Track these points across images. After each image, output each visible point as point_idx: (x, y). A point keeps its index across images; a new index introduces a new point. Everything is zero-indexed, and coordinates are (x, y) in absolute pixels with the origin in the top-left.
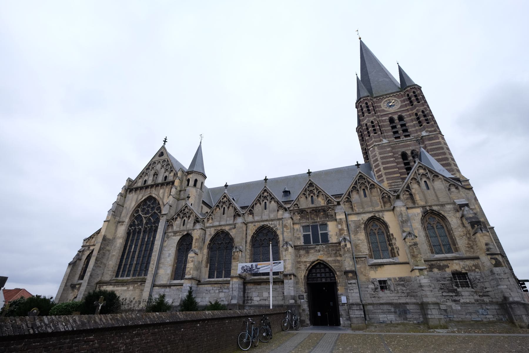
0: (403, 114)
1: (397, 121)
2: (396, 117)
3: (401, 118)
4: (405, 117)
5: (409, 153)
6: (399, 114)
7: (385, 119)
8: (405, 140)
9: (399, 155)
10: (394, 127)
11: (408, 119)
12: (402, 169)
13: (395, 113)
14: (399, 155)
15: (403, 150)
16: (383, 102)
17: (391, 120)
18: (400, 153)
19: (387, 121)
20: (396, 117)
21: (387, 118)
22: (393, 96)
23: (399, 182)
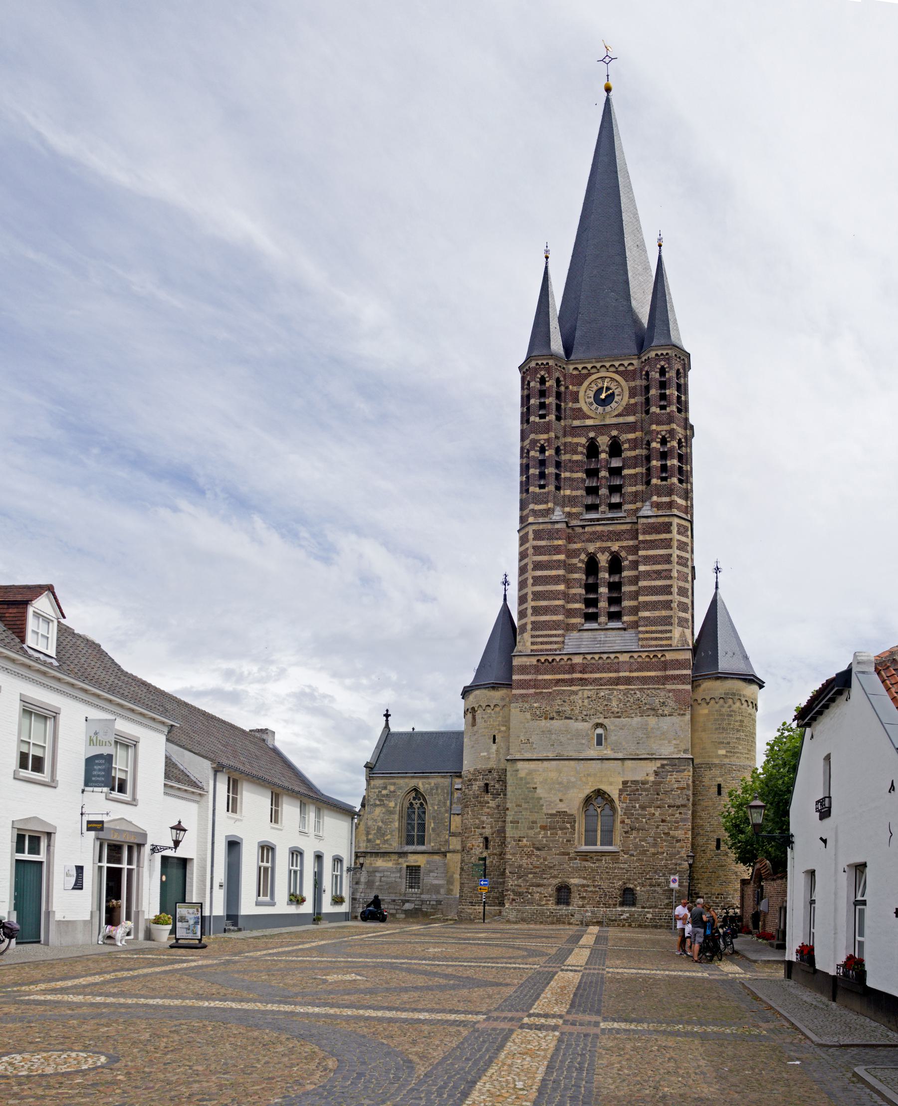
0: (624, 437)
2: (603, 441)
4: (626, 446)
5: (603, 559)
6: (614, 433)
7: (577, 444)
8: (608, 519)
9: (581, 561)
10: (592, 473)
11: (633, 453)
12: (577, 602)
13: (602, 429)
14: (580, 562)
15: (591, 548)
16: (586, 383)
17: (592, 450)
18: (583, 556)
19: (580, 449)
20: (603, 441)
21: (583, 440)
22: (613, 369)
23: (555, 636)
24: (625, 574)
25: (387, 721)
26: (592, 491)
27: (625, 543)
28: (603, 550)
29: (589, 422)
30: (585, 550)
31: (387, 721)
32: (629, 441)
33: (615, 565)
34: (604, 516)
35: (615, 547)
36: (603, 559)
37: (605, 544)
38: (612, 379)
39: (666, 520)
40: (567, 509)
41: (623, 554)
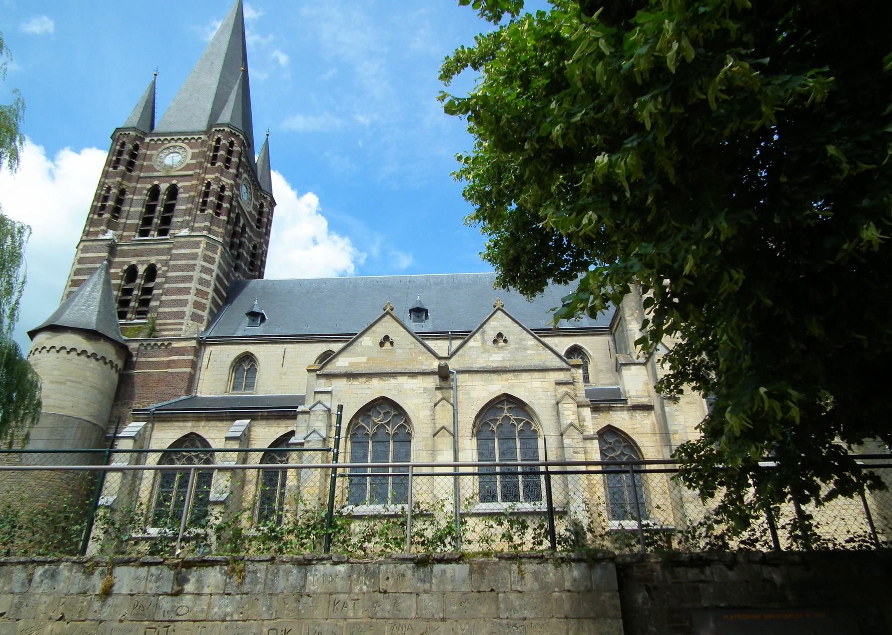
0: (179, 185)
1: (163, 197)
2: (164, 187)
3: (173, 192)
4: (181, 190)
5: (141, 269)
6: (174, 182)
10: (150, 209)
15: (133, 261)
17: (154, 192)
19: (145, 192)
20: (164, 187)
21: (149, 186)
24: (157, 280)
26: (147, 221)
27: (164, 258)
28: (142, 263)
29: (155, 174)
30: (125, 263)
32: (184, 187)
33: (151, 273)
34: (152, 238)
35: (153, 260)
36: (141, 269)
37: (144, 258)
38: (181, 147)
39: (198, 239)
40: (119, 232)
41: (159, 266)
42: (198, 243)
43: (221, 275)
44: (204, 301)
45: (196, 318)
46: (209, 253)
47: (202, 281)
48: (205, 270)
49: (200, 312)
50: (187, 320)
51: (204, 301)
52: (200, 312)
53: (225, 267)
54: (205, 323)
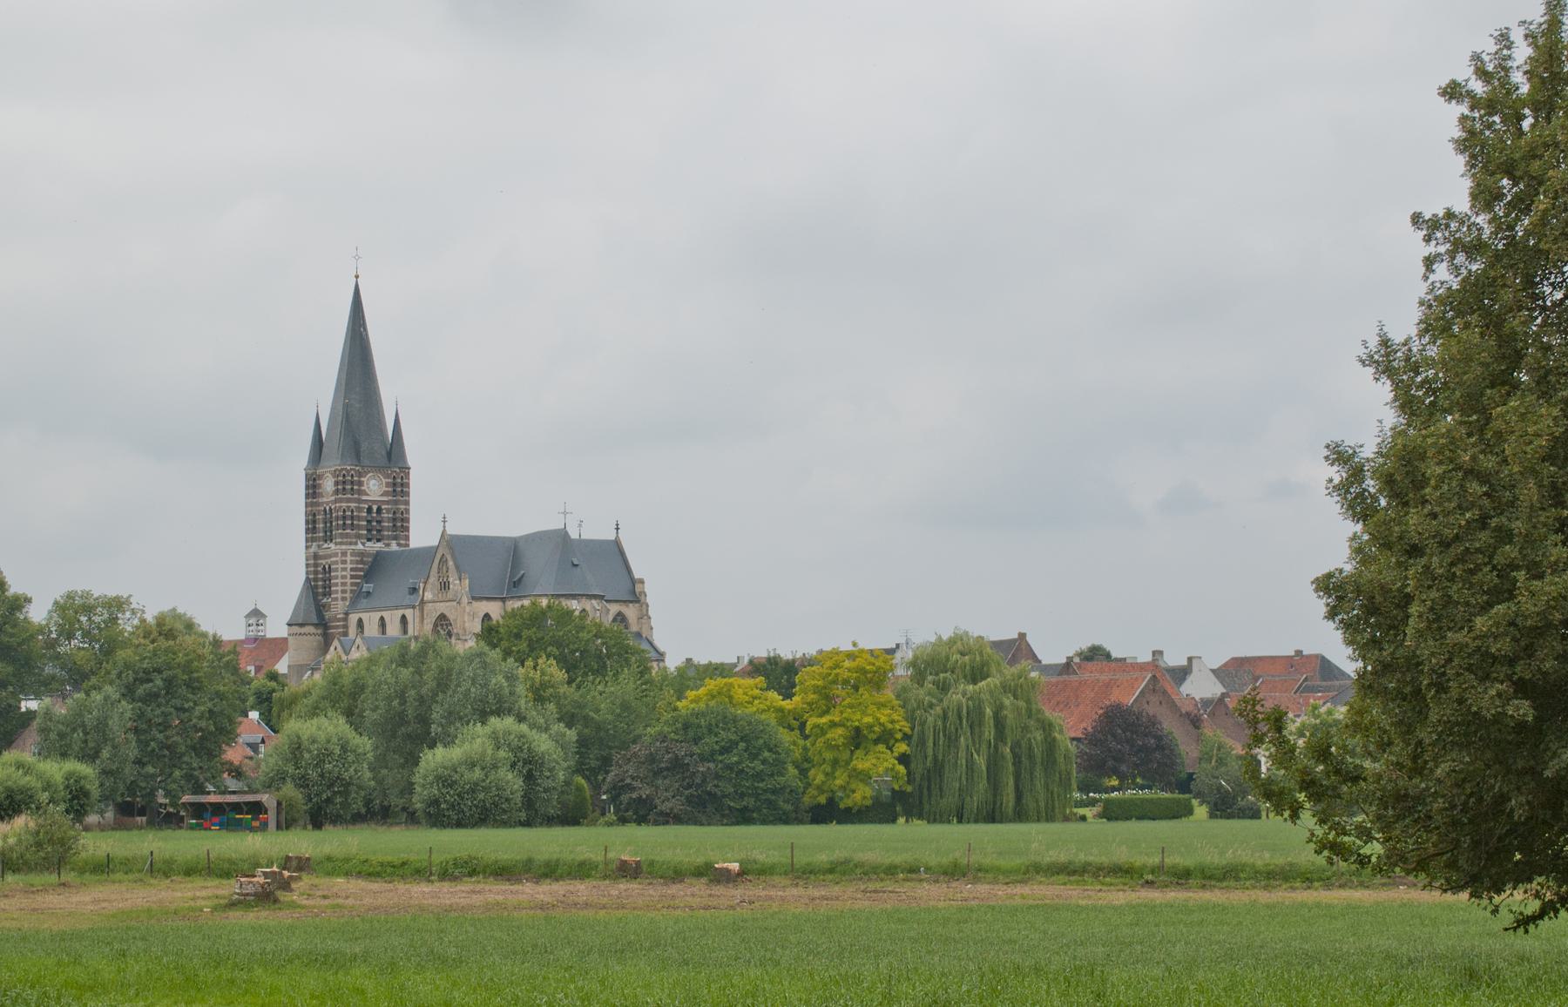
2: (328, 508)
5: (327, 567)
15: (324, 562)
25: (617, 533)
31: (617, 533)
42: (337, 553)
43: (354, 566)
44: (346, 588)
45: (344, 599)
46: (344, 558)
47: (344, 577)
48: (344, 569)
49: (344, 595)
50: (340, 602)
51: (346, 588)
52: (344, 595)
53: (357, 558)
54: (349, 600)
